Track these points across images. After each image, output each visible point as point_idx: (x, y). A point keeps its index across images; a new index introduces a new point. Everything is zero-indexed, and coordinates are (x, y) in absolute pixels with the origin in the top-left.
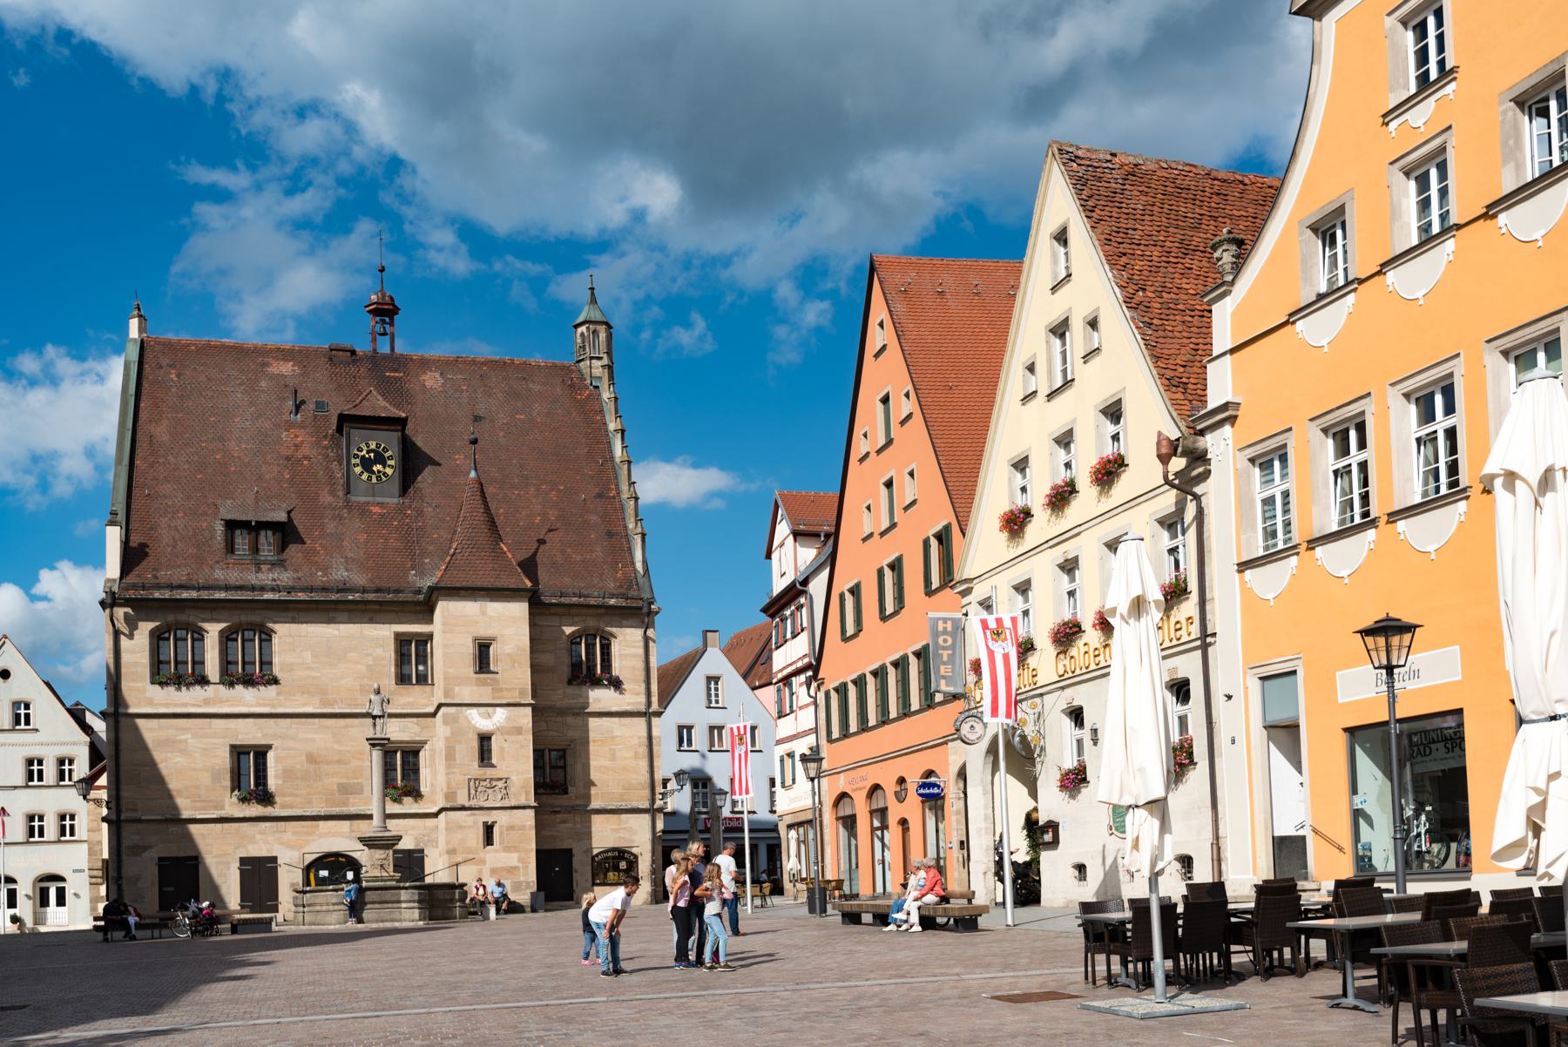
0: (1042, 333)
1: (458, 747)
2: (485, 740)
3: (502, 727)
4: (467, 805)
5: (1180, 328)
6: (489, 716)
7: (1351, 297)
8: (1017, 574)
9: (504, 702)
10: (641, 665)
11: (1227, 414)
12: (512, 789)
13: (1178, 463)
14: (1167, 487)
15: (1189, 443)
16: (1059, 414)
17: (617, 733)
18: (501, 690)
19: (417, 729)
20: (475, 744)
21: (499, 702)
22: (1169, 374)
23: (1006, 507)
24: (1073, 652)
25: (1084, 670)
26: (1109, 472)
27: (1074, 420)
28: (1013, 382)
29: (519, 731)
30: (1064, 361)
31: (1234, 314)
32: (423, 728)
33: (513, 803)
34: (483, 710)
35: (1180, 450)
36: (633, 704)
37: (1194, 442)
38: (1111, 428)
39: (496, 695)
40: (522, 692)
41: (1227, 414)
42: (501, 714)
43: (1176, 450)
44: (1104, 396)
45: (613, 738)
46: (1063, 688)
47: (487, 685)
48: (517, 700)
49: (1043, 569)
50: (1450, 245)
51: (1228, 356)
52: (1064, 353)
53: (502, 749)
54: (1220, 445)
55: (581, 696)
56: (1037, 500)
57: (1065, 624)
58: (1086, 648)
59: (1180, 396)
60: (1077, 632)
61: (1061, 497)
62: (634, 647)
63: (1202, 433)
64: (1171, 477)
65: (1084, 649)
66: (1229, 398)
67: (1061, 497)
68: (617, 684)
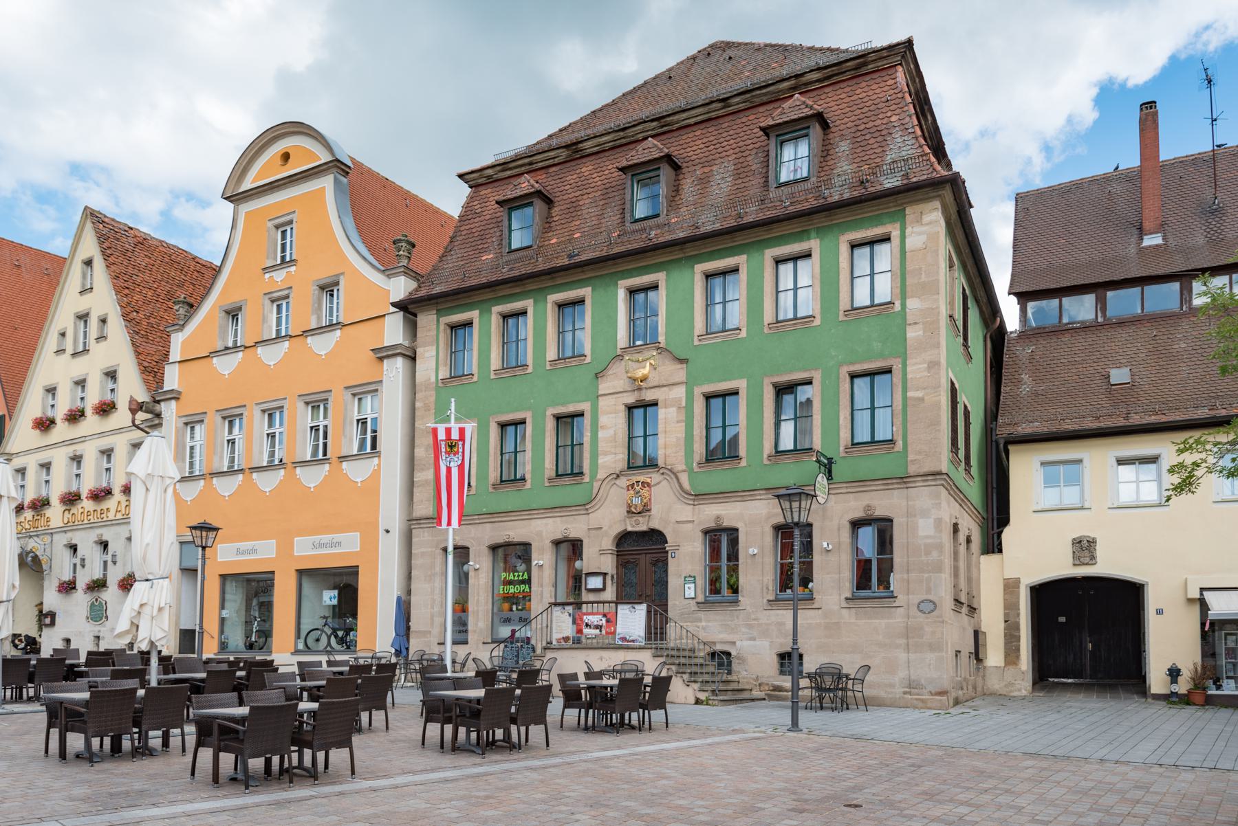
0: (72, 318)
5: (158, 340)
7: (241, 354)
8: (43, 456)
11: (175, 396)
13: (141, 416)
14: (134, 428)
15: (150, 406)
16: (79, 367)
22: (146, 364)
23: (39, 415)
24: (74, 510)
25: (80, 523)
26: (105, 409)
27: (87, 374)
28: (50, 342)
30: (85, 338)
31: (183, 342)
35: (144, 408)
37: (153, 406)
38: (111, 385)
41: (175, 396)
43: (141, 408)
44: (108, 364)
46: (65, 532)
49: (60, 459)
50: (286, 344)
51: (177, 364)
52: (85, 332)
54: (169, 410)
56: (60, 414)
57: (70, 493)
58: (82, 510)
59: (151, 378)
60: (76, 500)
61: (75, 416)
63: (158, 402)
64: (137, 422)
65: (81, 510)
66: (175, 387)
67: (75, 416)
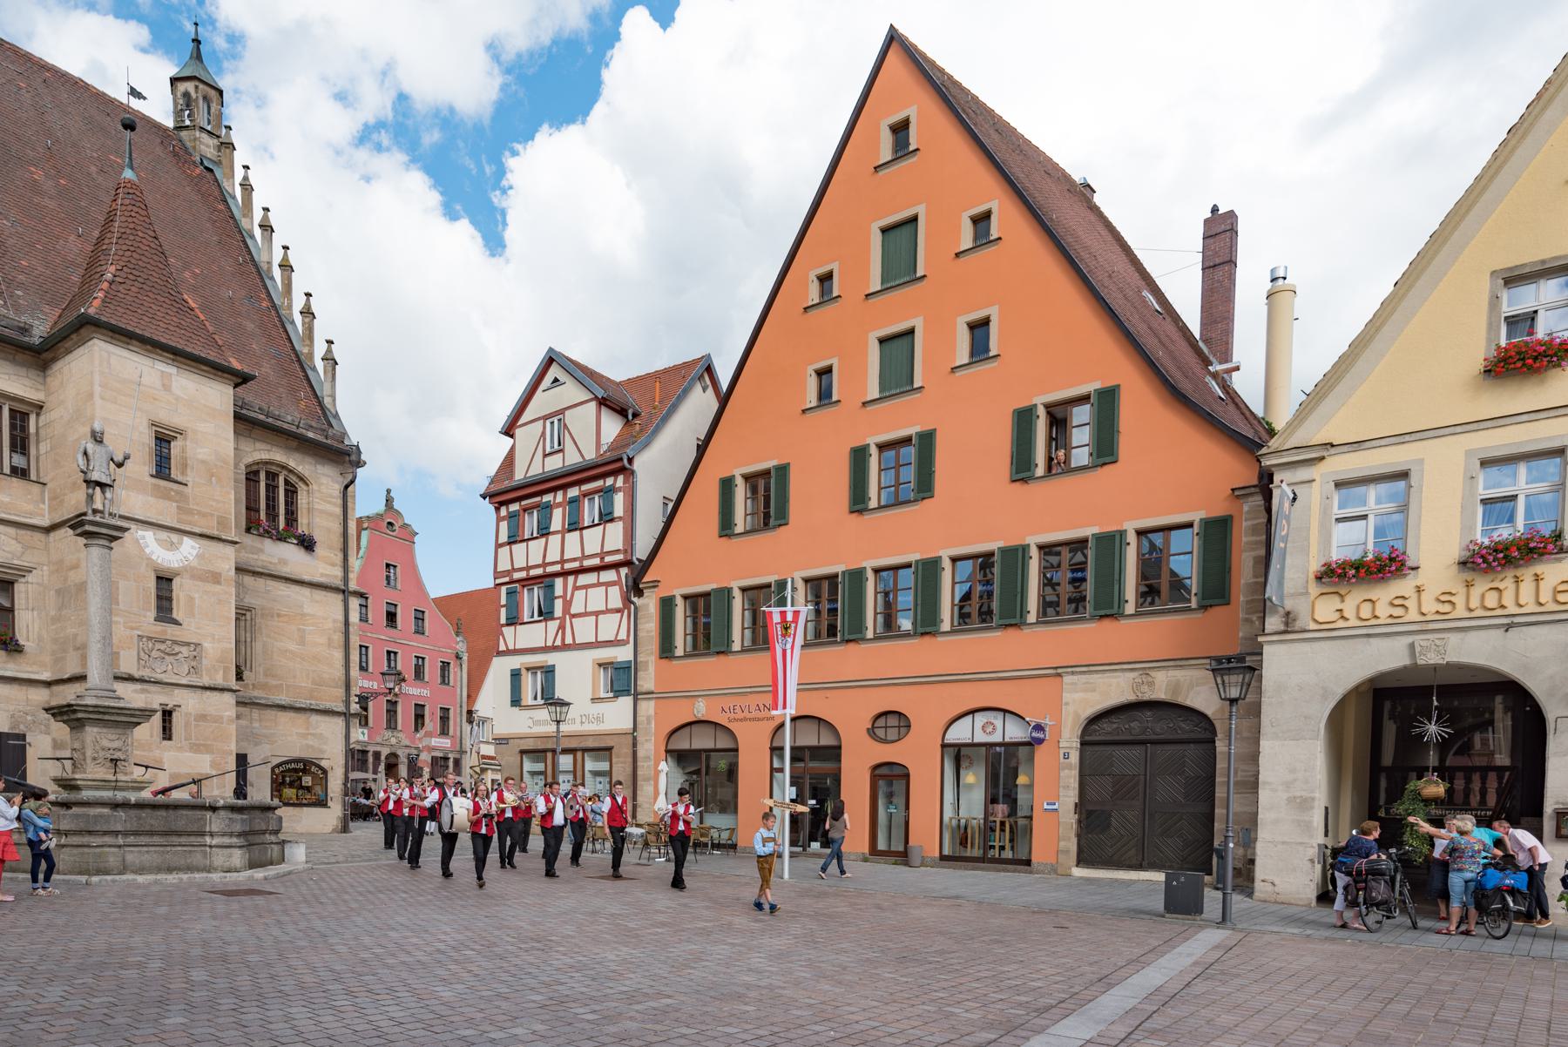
1: (122, 584)
2: (164, 581)
3: (193, 569)
4: (137, 675)
6: (172, 547)
9: (197, 530)
10: (338, 528)
12: (205, 662)
17: (308, 609)
18: (190, 512)
19: (15, 547)
20: (152, 584)
21: (188, 528)
29: (216, 578)
32: (26, 547)
33: (206, 681)
34: (164, 535)
36: (326, 575)
39: (184, 517)
40: (222, 522)
42: (189, 547)
45: (303, 615)
47: (169, 498)
48: (215, 533)
53: (191, 599)
55: (262, 551)
62: (329, 502)
68: (307, 544)
